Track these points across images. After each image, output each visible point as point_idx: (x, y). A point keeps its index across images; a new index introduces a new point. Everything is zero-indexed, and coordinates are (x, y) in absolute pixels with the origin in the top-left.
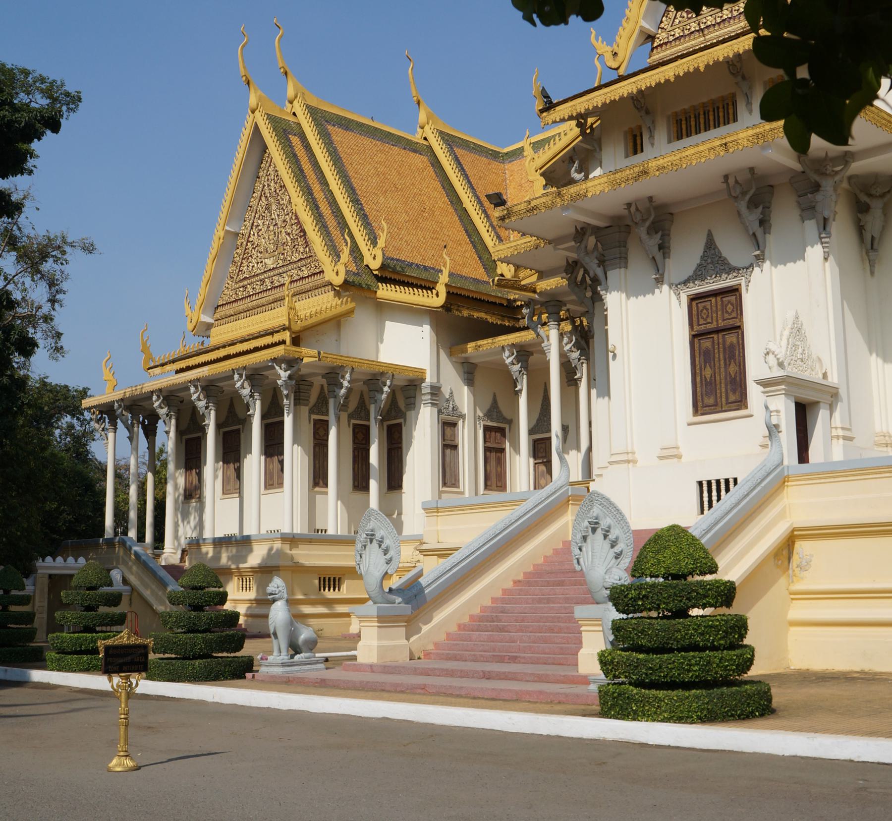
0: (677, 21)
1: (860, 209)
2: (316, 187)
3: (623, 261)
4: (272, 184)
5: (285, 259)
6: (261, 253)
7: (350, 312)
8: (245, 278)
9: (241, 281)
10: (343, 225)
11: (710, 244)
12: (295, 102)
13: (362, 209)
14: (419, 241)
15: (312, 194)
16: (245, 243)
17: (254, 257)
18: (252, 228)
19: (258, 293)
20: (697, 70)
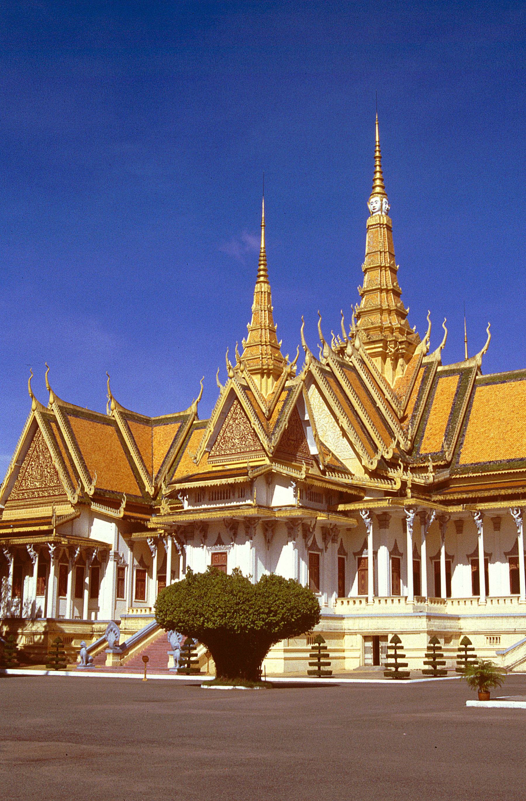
0: (218, 449)
1: (265, 530)
2: (63, 451)
4: (41, 446)
5: (46, 484)
6: (33, 478)
7: (78, 517)
8: (23, 490)
9: (21, 490)
10: (78, 477)
12: (53, 404)
13: (84, 463)
14: (110, 477)
15: (61, 455)
16: (24, 472)
17: (29, 480)
18: (28, 465)
19: (31, 498)
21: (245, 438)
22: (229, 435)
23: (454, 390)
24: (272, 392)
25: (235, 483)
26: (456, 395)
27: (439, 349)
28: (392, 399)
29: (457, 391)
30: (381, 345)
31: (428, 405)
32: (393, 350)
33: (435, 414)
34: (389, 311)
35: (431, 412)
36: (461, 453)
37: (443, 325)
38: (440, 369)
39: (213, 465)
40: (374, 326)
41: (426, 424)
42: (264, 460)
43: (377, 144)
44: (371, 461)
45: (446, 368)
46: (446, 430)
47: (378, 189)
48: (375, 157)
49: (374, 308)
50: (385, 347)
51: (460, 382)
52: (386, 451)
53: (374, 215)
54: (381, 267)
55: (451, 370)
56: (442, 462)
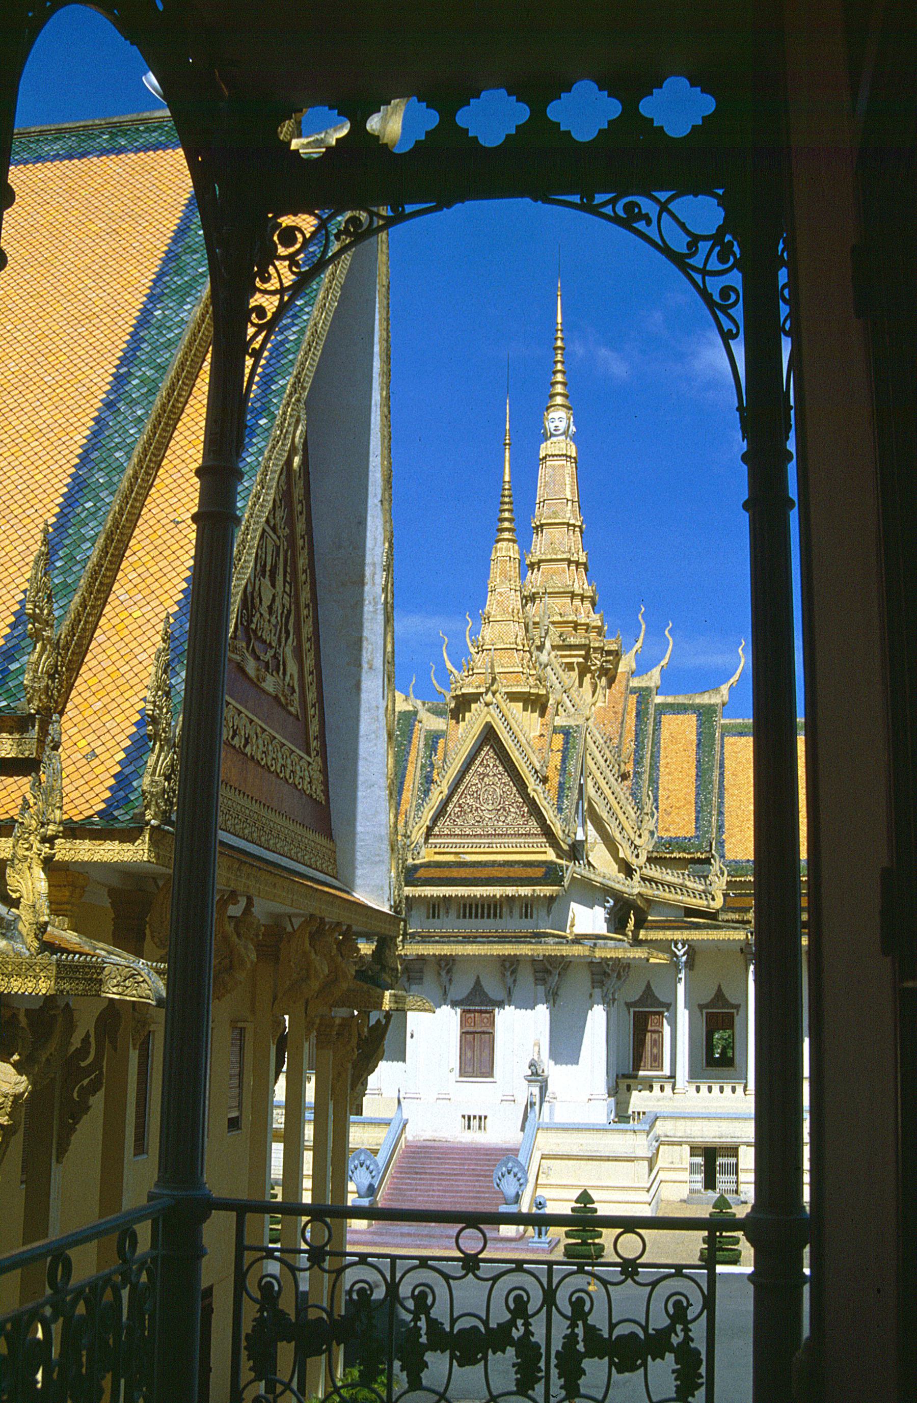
3: (420, 980)
11: (478, 982)
20: (495, 896)
21: (505, 810)
22: (471, 802)
23: (694, 737)
24: (538, 734)
25: (532, 895)
26: (698, 745)
27: (659, 668)
28: (606, 742)
29: (699, 740)
30: (583, 653)
31: (655, 756)
32: (598, 662)
33: (669, 774)
34: (583, 598)
35: (662, 769)
36: (724, 841)
37: (667, 633)
38: (659, 699)
39: (437, 850)
40: (565, 619)
41: (658, 788)
42: (545, 853)
43: (559, 327)
44: (636, 852)
45: (670, 700)
46: (696, 803)
47: (559, 400)
48: (556, 349)
49: (562, 590)
50: (587, 657)
51: (699, 727)
52: (638, 833)
53: (553, 439)
54: (568, 525)
55: (678, 704)
56: (702, 854)
